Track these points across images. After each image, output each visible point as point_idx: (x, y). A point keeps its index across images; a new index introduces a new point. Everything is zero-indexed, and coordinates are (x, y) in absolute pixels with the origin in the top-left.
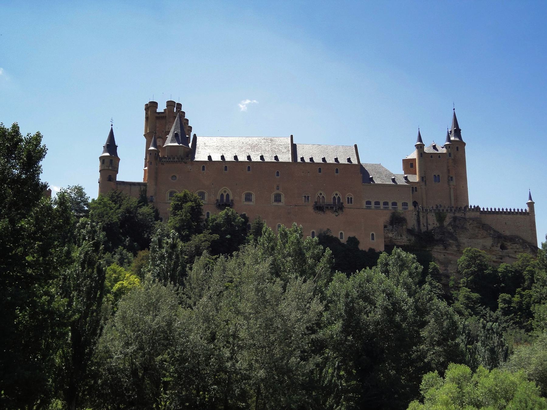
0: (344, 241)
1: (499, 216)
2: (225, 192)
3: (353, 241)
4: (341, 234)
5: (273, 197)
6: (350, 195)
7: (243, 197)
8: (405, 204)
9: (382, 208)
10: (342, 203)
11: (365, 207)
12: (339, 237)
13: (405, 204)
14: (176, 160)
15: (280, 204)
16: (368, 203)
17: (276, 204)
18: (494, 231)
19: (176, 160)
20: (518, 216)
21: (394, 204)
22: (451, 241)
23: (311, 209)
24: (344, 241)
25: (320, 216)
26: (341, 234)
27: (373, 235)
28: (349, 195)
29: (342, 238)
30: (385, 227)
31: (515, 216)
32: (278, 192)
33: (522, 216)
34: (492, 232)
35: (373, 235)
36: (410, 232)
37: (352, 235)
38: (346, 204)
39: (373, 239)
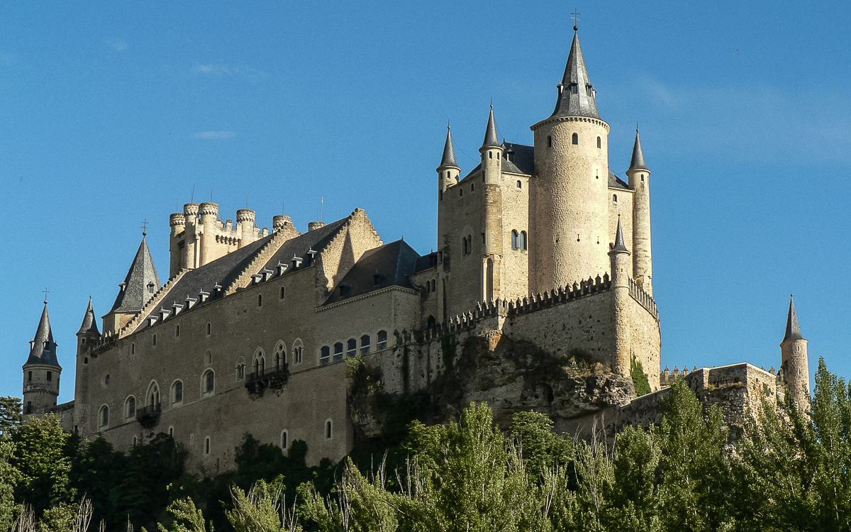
0: (285, 451)
1: (552, 310)
2: (156, 389)
3: (300, 448)
4: (285, 434)
5: (204, 380)
6: (298, 343)
7: (173, 392)
8: (382, 335)
9: (344, 357)
10: (288, 364)
11: (318, 364)
12: (281, 446)
13: (382, 335)
14: (105, 343)
15: (212, 394)
16: (325, 351)
17: (207, 395)
18: (540, 355)
19: (105, 343)
20: (589, 298)
21: (366, 340)
22: (449, 406)
23: (244, 394)
24: (285, 451)
25: (259, 403)
26: (285, 434)
27: (329, 423)
28: (298, 342)
29: (285, 446)
30: (349, 400)
31: (582, 301)
32: (208, 367)
33: (597, 298)
34: (529, 361)
35: (329, 423)
36: (383, 401)
37: (298, 434)
38: (293, 366)
39: (329, 436)
